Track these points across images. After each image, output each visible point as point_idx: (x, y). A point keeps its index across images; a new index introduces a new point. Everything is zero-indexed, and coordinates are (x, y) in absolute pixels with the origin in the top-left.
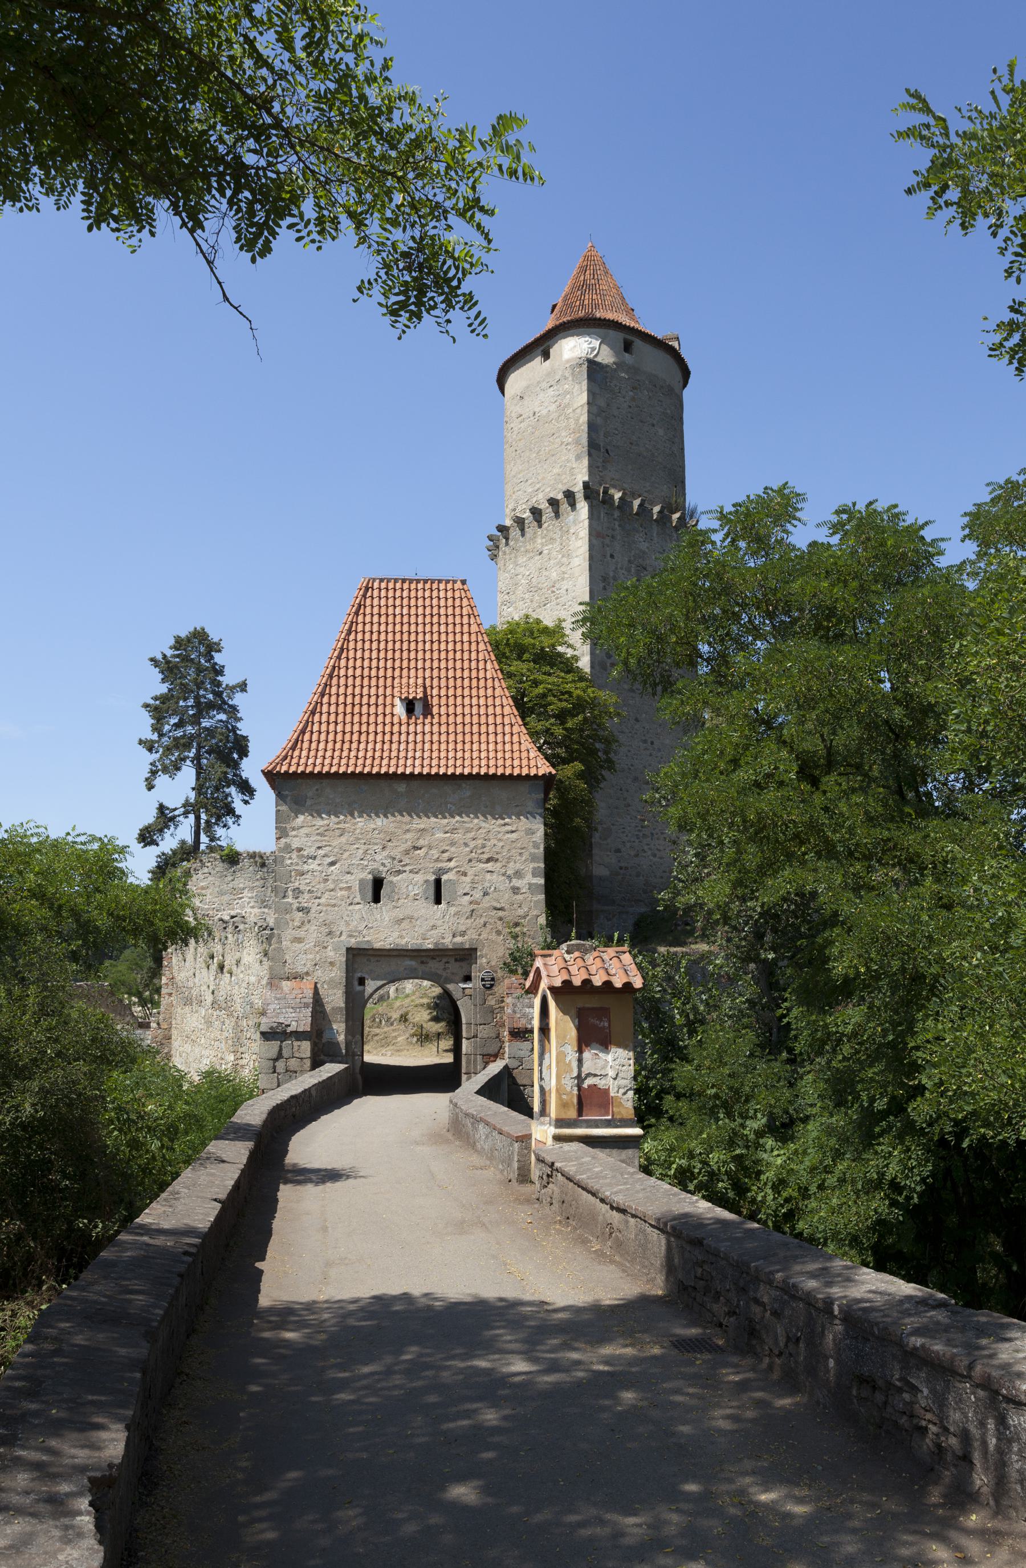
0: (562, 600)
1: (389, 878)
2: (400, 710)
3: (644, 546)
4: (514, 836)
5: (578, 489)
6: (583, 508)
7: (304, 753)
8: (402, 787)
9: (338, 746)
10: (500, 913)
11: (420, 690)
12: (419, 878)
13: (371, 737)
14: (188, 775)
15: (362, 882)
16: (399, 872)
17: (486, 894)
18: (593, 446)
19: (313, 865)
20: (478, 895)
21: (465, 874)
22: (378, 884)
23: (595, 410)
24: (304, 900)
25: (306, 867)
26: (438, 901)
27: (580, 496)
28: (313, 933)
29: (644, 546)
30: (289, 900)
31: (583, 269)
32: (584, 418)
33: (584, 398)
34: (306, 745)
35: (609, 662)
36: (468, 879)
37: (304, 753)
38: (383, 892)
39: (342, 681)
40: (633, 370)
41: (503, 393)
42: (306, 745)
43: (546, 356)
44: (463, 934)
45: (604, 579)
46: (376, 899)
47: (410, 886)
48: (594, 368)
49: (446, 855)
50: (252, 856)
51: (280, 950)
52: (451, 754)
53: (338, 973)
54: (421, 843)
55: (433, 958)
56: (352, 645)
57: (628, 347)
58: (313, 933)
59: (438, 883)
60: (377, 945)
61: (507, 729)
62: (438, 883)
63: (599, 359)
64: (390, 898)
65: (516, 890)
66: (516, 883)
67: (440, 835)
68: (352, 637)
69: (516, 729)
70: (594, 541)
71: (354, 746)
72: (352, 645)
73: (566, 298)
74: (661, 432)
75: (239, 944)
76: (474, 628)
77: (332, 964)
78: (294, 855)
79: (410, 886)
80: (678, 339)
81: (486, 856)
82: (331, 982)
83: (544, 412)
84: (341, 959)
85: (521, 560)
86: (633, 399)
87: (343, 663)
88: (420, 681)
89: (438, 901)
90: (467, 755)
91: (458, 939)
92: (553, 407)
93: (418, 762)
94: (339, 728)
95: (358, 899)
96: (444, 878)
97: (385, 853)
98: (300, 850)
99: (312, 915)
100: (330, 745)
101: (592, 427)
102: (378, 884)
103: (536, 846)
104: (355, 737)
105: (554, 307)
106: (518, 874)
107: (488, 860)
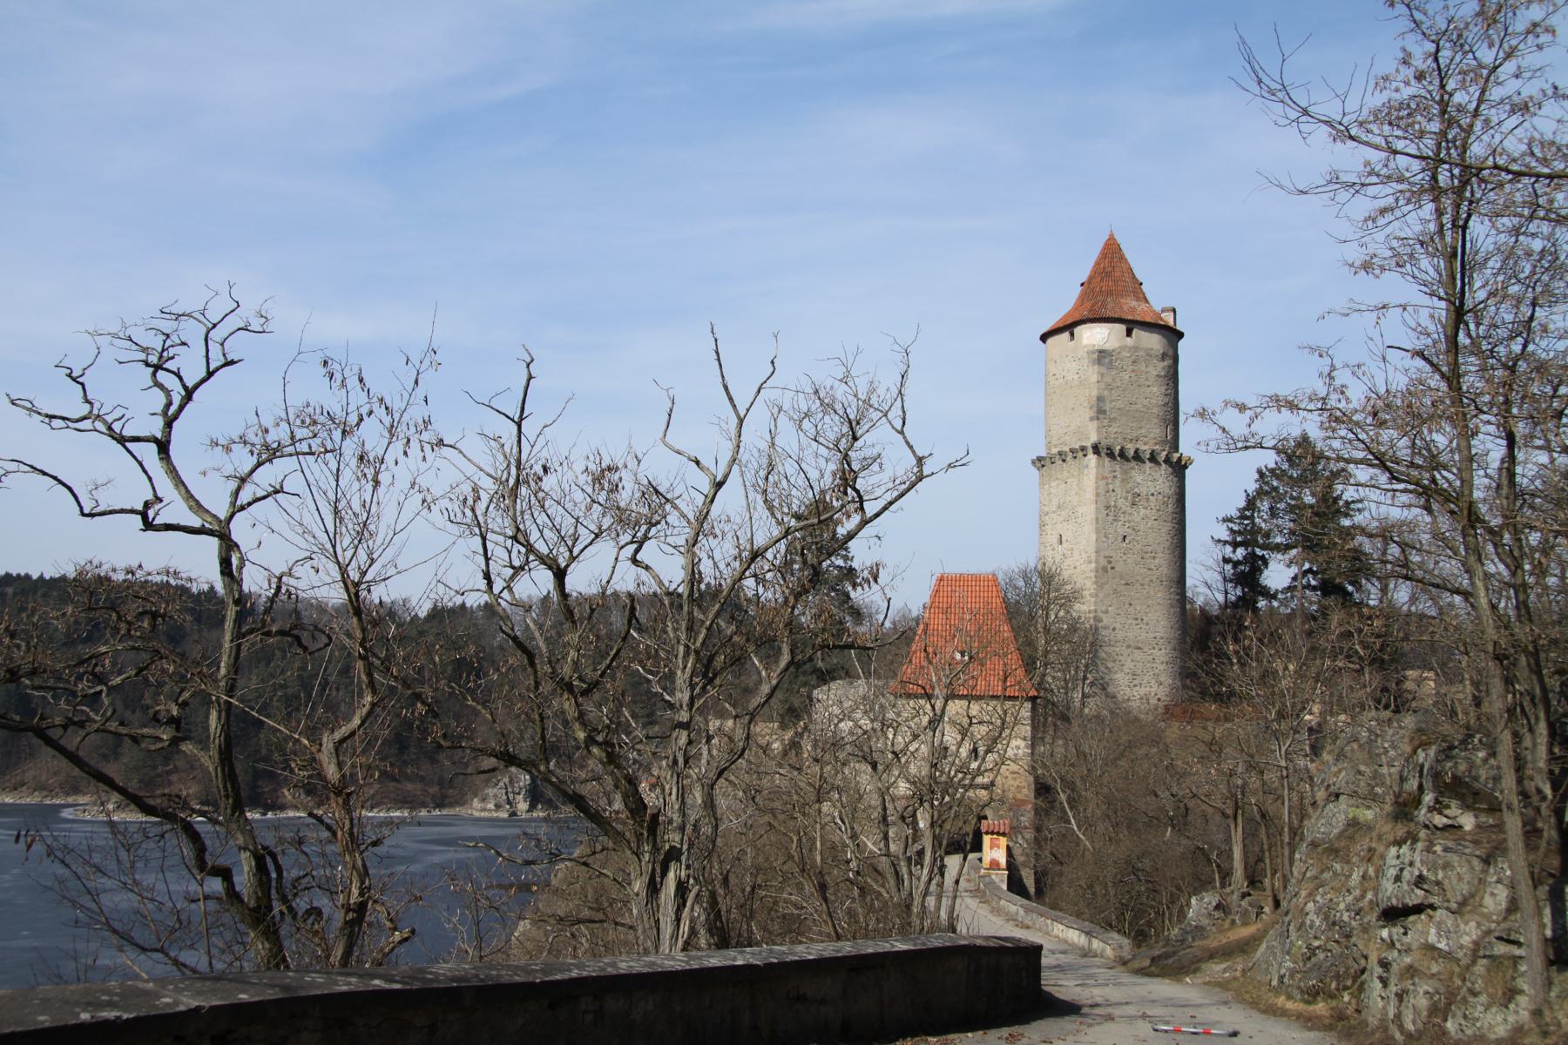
3: (1139, 479)
6: (1092, 458)
23: (1102, 385)
27: (1090, 451)
29: (1139, 479)
32: (1095, 393)
33: (1094, 378)
40: (1136, 349)
43: (1072, 335)
45: (1108, 507)
48: (1102, 356)
57: (1129, 333)
63: (1108, 347)
80: (1174, 311)
85: (1054, 484)
101: (1100, 399)
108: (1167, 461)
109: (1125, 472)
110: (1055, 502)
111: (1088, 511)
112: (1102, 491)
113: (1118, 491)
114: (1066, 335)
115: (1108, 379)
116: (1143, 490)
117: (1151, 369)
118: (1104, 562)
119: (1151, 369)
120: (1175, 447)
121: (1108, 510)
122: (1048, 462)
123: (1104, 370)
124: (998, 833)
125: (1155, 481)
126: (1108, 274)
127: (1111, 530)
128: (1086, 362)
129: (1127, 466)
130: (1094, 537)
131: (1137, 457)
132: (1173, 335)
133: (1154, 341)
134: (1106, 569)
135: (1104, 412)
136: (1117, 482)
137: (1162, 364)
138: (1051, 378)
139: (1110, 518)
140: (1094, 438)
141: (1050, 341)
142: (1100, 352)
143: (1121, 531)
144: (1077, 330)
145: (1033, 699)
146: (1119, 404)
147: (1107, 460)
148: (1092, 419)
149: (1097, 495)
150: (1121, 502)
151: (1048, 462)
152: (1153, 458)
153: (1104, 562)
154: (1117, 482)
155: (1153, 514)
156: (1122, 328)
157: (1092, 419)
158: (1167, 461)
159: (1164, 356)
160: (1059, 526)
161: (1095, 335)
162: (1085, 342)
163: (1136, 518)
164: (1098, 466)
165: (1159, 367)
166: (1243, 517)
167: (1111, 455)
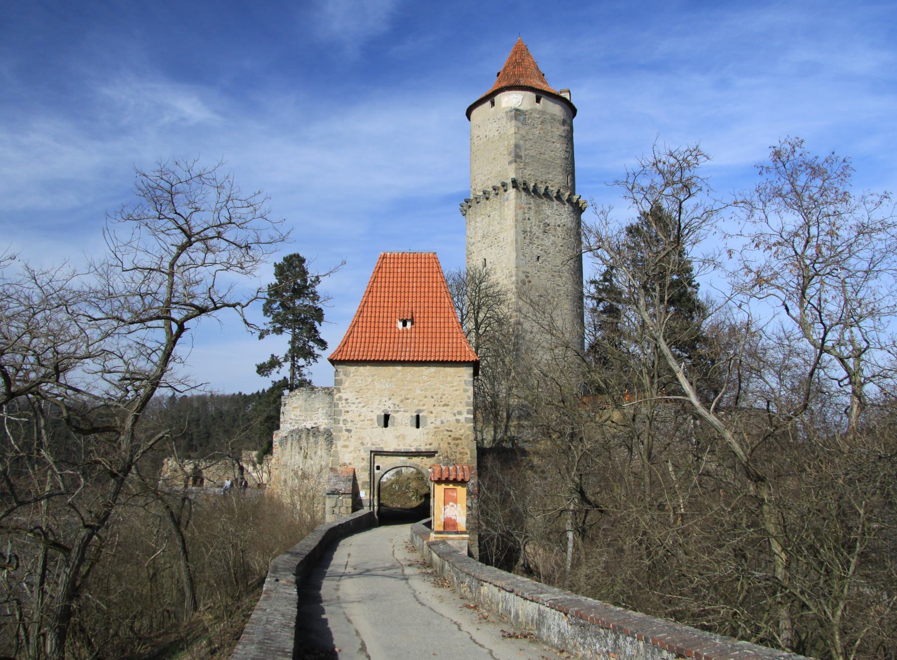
0: (501, 244)
1: (392, 414)
2: (400, 325)
3: (549, 212)
4: (457, 393)
5: (509, 181)
6: (512, 192)
7: (349, 349)
8: (399, 368)
9: (367, 345)
10: (450, 433)
11: (410, 314)
12: (408, 415)
13: (384, 340)
14: (287, 336)
15: (378, 417)
16: (398, 411)
17: (442, 422)
18: (517, 157)
19: (353, 407)
20: (438, 423)
21: (432, 413)
22: (387, 417)
23: (519, 136)
24: (349, 426)
25: (349, 409)
26: (418, 427)
27: (510, 186)
28: (353, 443)
29: (549, 212)
30: (341, 424)
31: (516, 53)
32: (512, 142)
33: (512, 130)
34: (350, 344)
35: (527, 280)
36: (433, 415)
37: (349, 349)
38: (389, 422)
39: (369, 309)
40: (543, 113)
41: (469, 119)
42: (350, 344)
43: (493, 104)
44: (430, 444)
45: (525, 232)
46: (386, 425)
47: (402, 419)
48: (517, 114)
49: (422, 403)
50: (324, 389)
51: (336, 451)
52: (425, 350)
53: (366, 464)
54: (409, 396)
55: (415, 456)
56: (375, 289)
57: (538, 101)
58: (353, 443)
59: (418, 417)
60: (385, 450)
61: (455, 335)
62: (418, 417)
63: (521, 108)
64: (393, 425)
65: (458, 421)
66: (458, 417)
67: (418, 392)
68: (375, 285)
69: (459, 335)
70: (519, 211)
71: (375, 345)
72: (375, 289)
73: (505, 70)
74: (558, 146)
75: (316, 443)
76: (439, 279)
77: (363, 459)
78: (344, 402)
79: (402, 419)
81: (442, 403)
82: (363, 469)
83: (491, 136)
84: (367, 456)
86: (541, 129)
87: (370, 299)
88: (410, 309)
89: (418, 427)
90: (433, 350)
91: (428, 447)
92: (496, 134)
93: (407, 354)
94: (367, 335)
95: (376, 425)
96: (421, 415)
97: (391, 401)
98: (346, 400)
99: (353, 433)
100: (363, 345)
101: (517, 146)
102: (387, 417)
103: (469, 398)
104: (376, 340)
105: (499, 74)
106: (460, 413)
107: (444, 405)
108: (569, 200)
109: (538, 206)
110: (480, 234)
111: (508, 234)
112: (520, 218)
113: (533, 220)
114: (488, 103)
115: (523, 132)
116: (551, 221)
117: (554, 129)
118: (523, 276)
119: (554, 129)
120: (573, 193)
121: (525, 235)
122: (474, 203)
123: (520, 125)
124: (455, 482)
125: (559, 215)
126: (519, 64)
127: (528, 250)
128: (504, 121)
129: (539, 201)
130: (515, 256)
131: (547, 195)
132: (572, 110)
133: (556, 110)
134: (524, 284)
135: (520, 157)
136: (532, 212)
137: (563, 128)
138: (476, 140)
139: (527, 241)
140: (511, 174)
141: (475, 113)
142: (517, 110)
143: (537, 252)
144: (496, 98)
145: (475, 366)
146: (532, 153)
147: (523, 194)
148: (510, 163)
149: (517, 221)
150: (535, 229)
151: (474, 203)
152: (559, 197)
153: (523, 276)
154: (532, 212)
155: (559, 241)
156: (532, 95)
157: (510, 163)
158: (569, 200)
159: (564, 122)
160: (484, 252)
161: (511, 100)
162: (504, 105)
163: (547, 242)
164: (517, 198)
165: (561, 130)
166: (605, 280)
167: (526, 190)
